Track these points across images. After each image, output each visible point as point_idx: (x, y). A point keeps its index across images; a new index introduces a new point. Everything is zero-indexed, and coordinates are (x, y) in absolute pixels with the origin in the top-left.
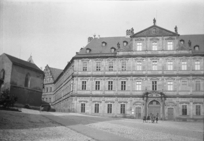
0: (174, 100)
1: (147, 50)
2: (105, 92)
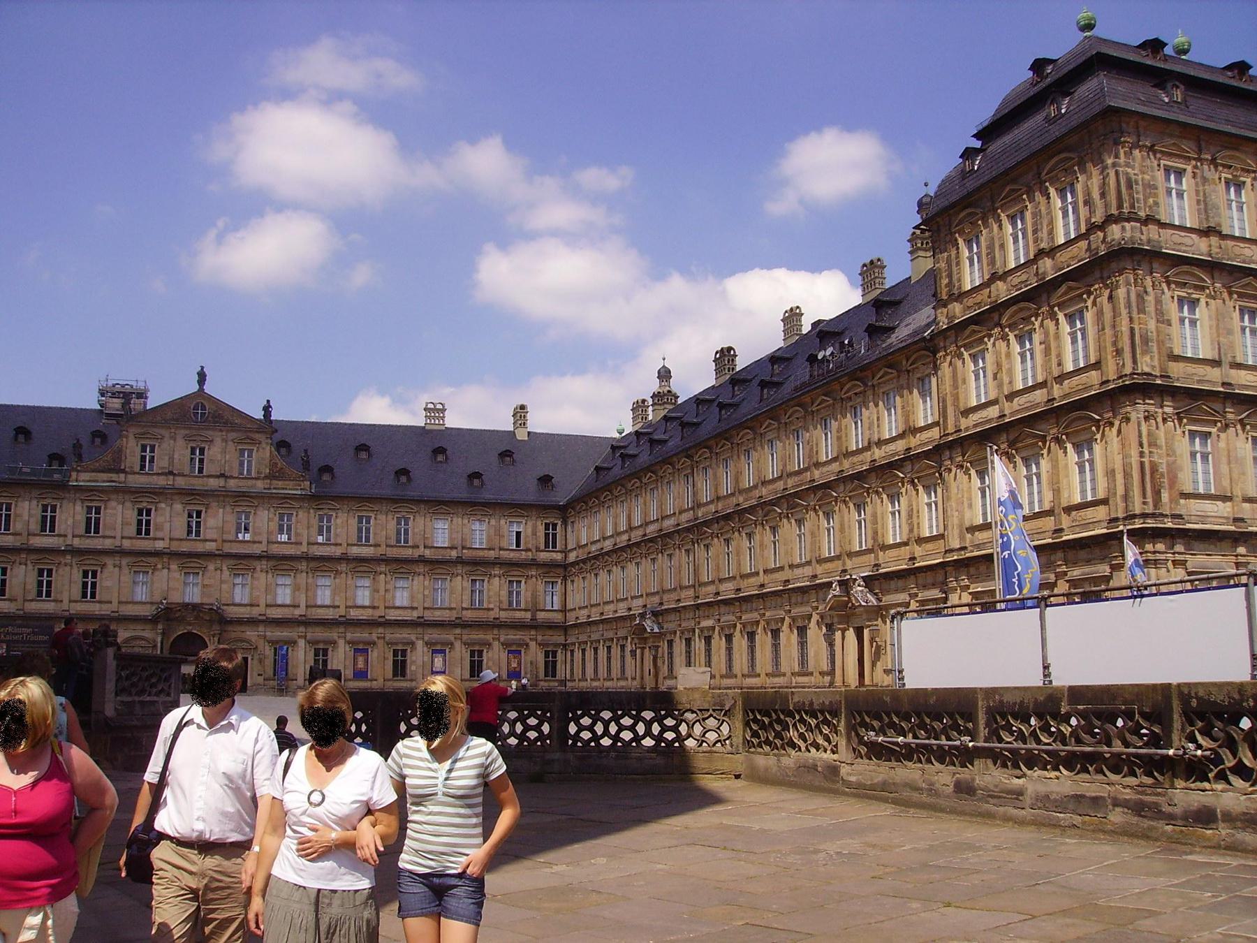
0: (251, 634)
1: (171, 473)
2: (27, 604)
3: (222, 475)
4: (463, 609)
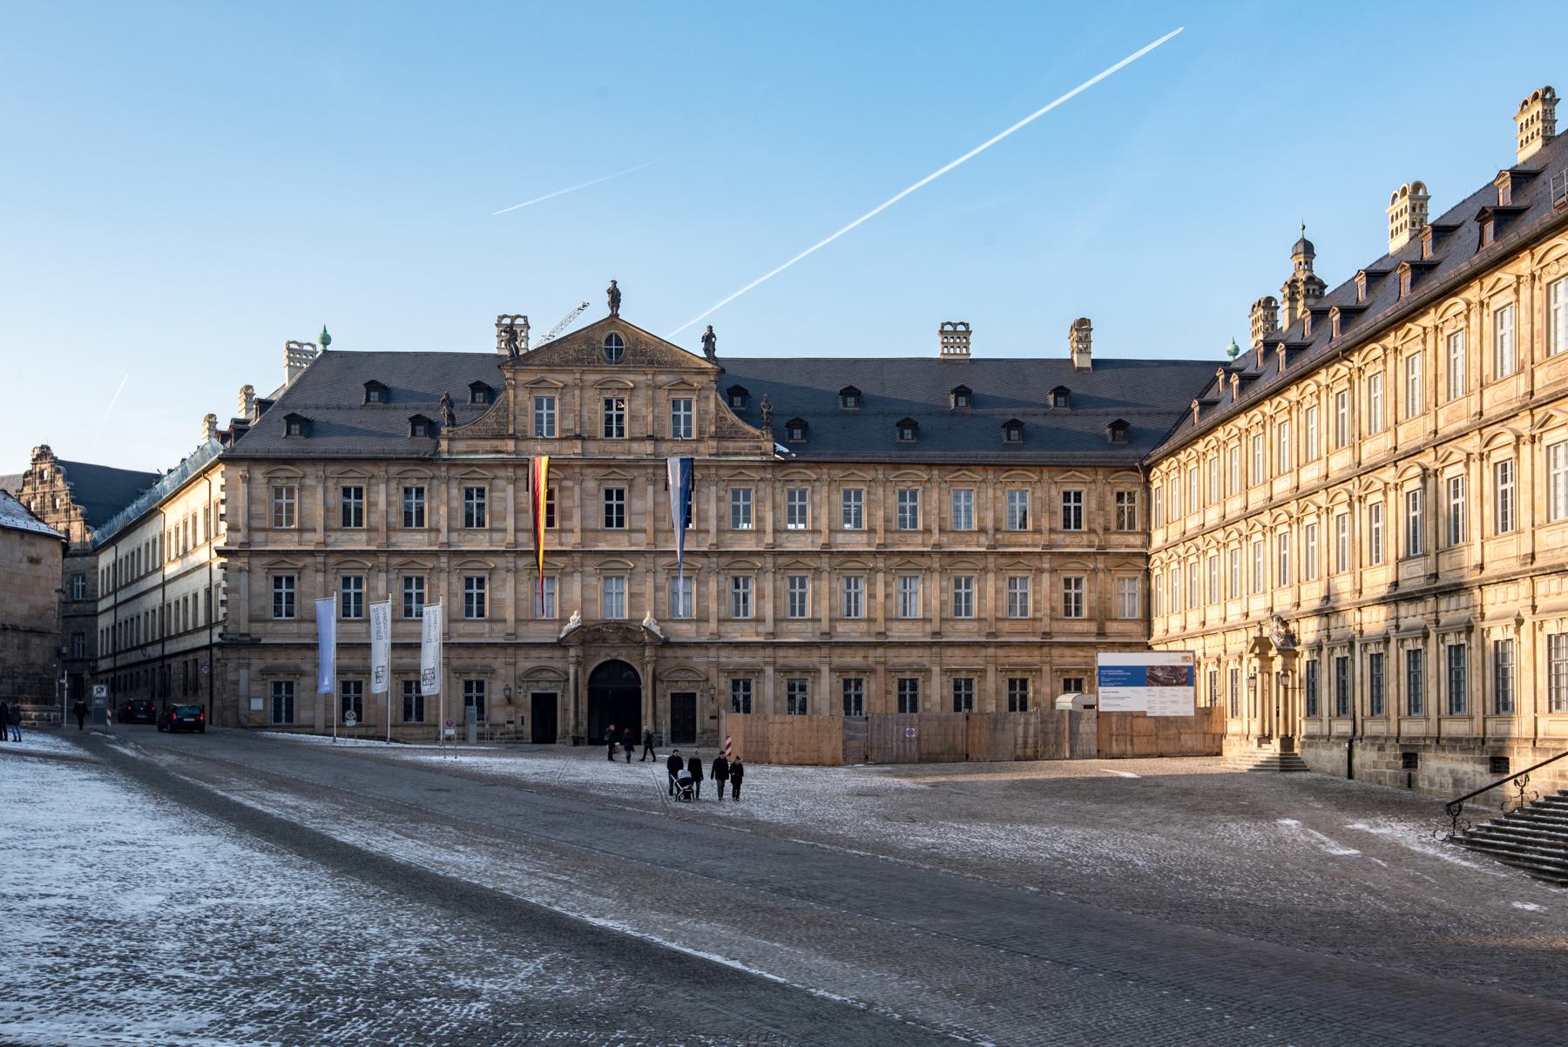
0: (698, 659)
3: (650, 438)
4: (997, 619)
